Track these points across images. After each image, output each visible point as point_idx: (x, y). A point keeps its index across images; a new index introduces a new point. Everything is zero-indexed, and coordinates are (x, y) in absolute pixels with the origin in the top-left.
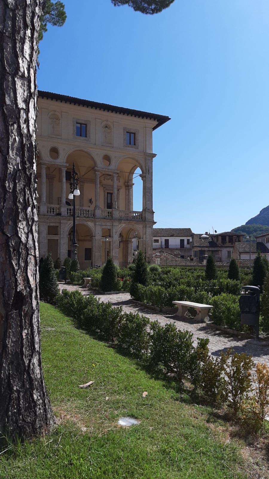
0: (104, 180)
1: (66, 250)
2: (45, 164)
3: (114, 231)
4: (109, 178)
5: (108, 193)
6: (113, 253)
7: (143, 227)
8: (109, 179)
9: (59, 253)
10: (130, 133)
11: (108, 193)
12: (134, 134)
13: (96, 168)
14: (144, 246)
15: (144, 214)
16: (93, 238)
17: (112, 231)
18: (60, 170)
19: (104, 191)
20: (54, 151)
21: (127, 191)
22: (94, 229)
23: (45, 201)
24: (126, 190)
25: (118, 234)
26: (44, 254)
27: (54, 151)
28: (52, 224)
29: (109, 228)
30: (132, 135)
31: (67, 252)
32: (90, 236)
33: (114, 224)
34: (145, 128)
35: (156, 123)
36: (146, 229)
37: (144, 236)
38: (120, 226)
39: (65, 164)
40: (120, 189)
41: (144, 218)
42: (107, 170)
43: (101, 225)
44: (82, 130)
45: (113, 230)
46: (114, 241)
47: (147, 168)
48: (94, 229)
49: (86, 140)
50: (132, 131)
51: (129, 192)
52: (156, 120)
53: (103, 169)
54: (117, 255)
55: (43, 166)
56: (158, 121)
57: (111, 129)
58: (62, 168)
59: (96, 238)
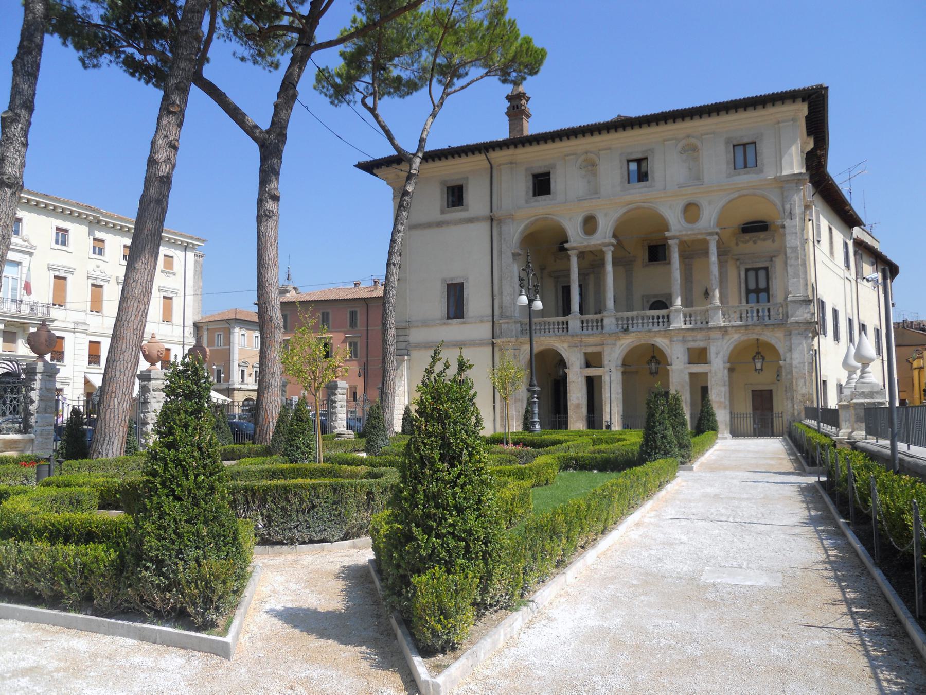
0: (737, 244)
1: (618, 394)
2: (573, 248)
8: (747, 242)
10: (745, 145)
11: (747, 270)
13: (667, 234)
14: (789, 376)
18: (602, 253)
19: (738, 268)
20: (590, 224)
22: (669, 350)
27: (590, 224)
28: (590, 350)
29: (701, 344)
36: (790, 339)
37: (788, 355)
38: (727, 337)
40: (774, 256)
43: (684, 341)
47: (788, 207)
50: (746, 140)
54: (723, 400)
56: (803, 101)
58: (604, 249)
59: (674, 367)
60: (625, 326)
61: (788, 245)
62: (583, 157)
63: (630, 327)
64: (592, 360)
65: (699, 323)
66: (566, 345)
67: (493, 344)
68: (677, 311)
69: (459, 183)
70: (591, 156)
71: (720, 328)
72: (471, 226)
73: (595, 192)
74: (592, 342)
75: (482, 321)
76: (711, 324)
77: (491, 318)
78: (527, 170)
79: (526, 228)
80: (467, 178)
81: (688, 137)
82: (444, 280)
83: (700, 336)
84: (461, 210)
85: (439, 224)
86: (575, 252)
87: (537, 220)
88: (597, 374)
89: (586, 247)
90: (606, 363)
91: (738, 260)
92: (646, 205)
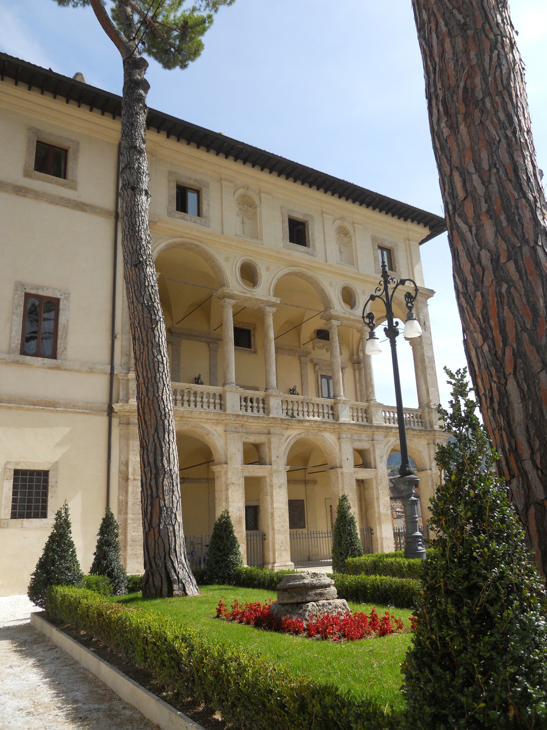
2: (231, 297)
3: (378, 452)
4: (322, 344)
5: (323, 377)
6: (379, 507)
7: (429, 444)
8: (320, 348)
9: (269, 510)
12: (389, 251)
15: (427, 414)
16: (339, 470)
17: (372, 453)
20: (249, 274)
21: (357, 373)
23: (234, 380)
24: (354, 370)
25: (385, 459)
26: (238, 515)
28: (252, 439)
30: (385, 253)
31: (286, 507)
32: (329, 467)
33: (375, 436)
34: (407, 242)
35: (426, 232)
38: (386, 440)
39: (274, 299)
41: (428, 423)
42: (352, 317)
43: (353, 441)
44: (298, 232)
45: (374, 450)
46: (379, 478)
48: (337, 450)
49: (308, 253)
50: (387, 244)
51: (360, 375)
52: (428, 227)
53: (344, 313)
55: (227, 300)
57: (351, 236)
59: (345, 470)
60: (290, 412)
61: (426, 354)
62: (241, 191)
63: (295, 415)
64: (254, 454)
65: (360, 419)
66: (220, 429)
67: (110, 411)
68: (344, 402)
69: (65, 144)
70: (250, 193)
71: (387, 427)
72: (78, 214)
73: (256, 235)
74: (254, 428)
75: (91, 371)
76: (375, 422)
77: (109, 367)
78: (170, 173)
79: (170, 247)
80: (78, 143)
81: (342, 218)
82: (19, 285)
83: (364, 436)
84: (63, 185)
85: (20, 191)
86: (233, 302)
87: (182, 244)
88: (260, 475)
89: (246, 299)
90: (274, 459)
91: (317, 364)
92: (309, 273)
